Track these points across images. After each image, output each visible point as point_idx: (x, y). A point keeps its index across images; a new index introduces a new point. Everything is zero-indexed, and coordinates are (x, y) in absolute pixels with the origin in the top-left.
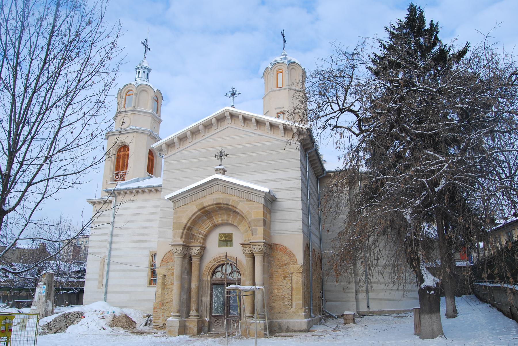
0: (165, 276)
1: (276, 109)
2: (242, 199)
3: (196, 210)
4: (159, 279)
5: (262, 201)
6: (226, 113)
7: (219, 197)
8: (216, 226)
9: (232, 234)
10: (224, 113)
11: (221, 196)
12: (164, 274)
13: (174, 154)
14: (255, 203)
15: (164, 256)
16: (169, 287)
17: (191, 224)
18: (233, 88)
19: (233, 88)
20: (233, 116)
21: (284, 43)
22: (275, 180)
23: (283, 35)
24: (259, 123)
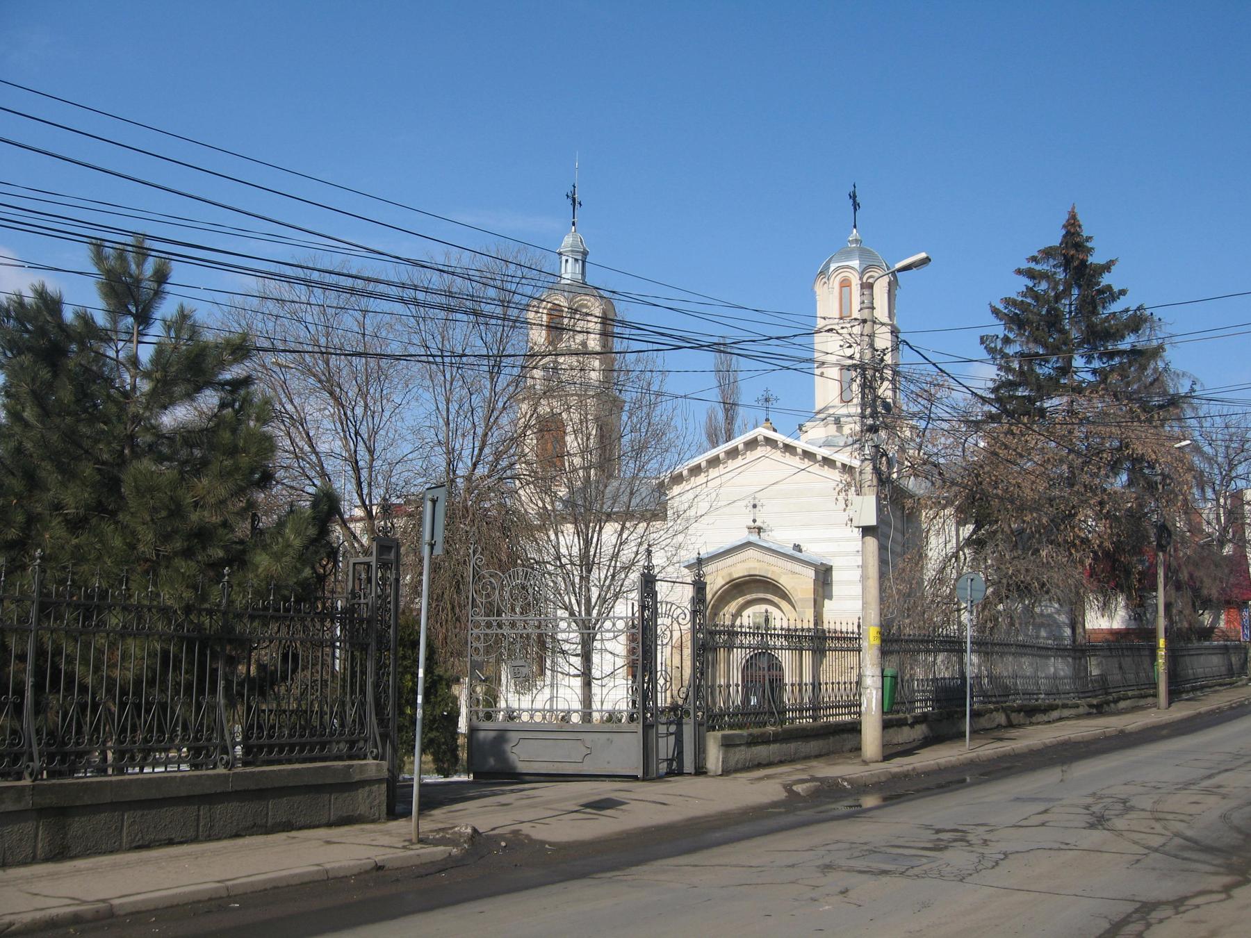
3: (723, 583)
5: (811, 573)
8: (749, 604)
11: (756, 565)
17: (715, 601)
18: (767, 391)
19: (767, 391)
20: (769, 442)
21: (855, 210)
22: (830, 540)
24: (807, 455)
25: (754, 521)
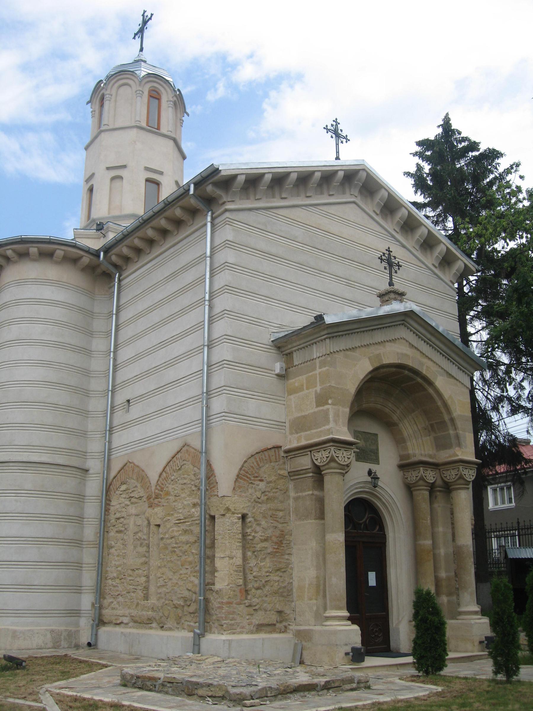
0: (244, 517)
1: (147, 169)
2: (440, 370)
4: (233, 524)
6: (361, 172)
7: (405, 352)
9: (376, 435)
10: (359, 170)
12: (245, 511)
13: (250, 210)
14: (458, 383)
15: (243, 466)
16: (258, 547)
23: (145, 22)
25: (391, 284)
